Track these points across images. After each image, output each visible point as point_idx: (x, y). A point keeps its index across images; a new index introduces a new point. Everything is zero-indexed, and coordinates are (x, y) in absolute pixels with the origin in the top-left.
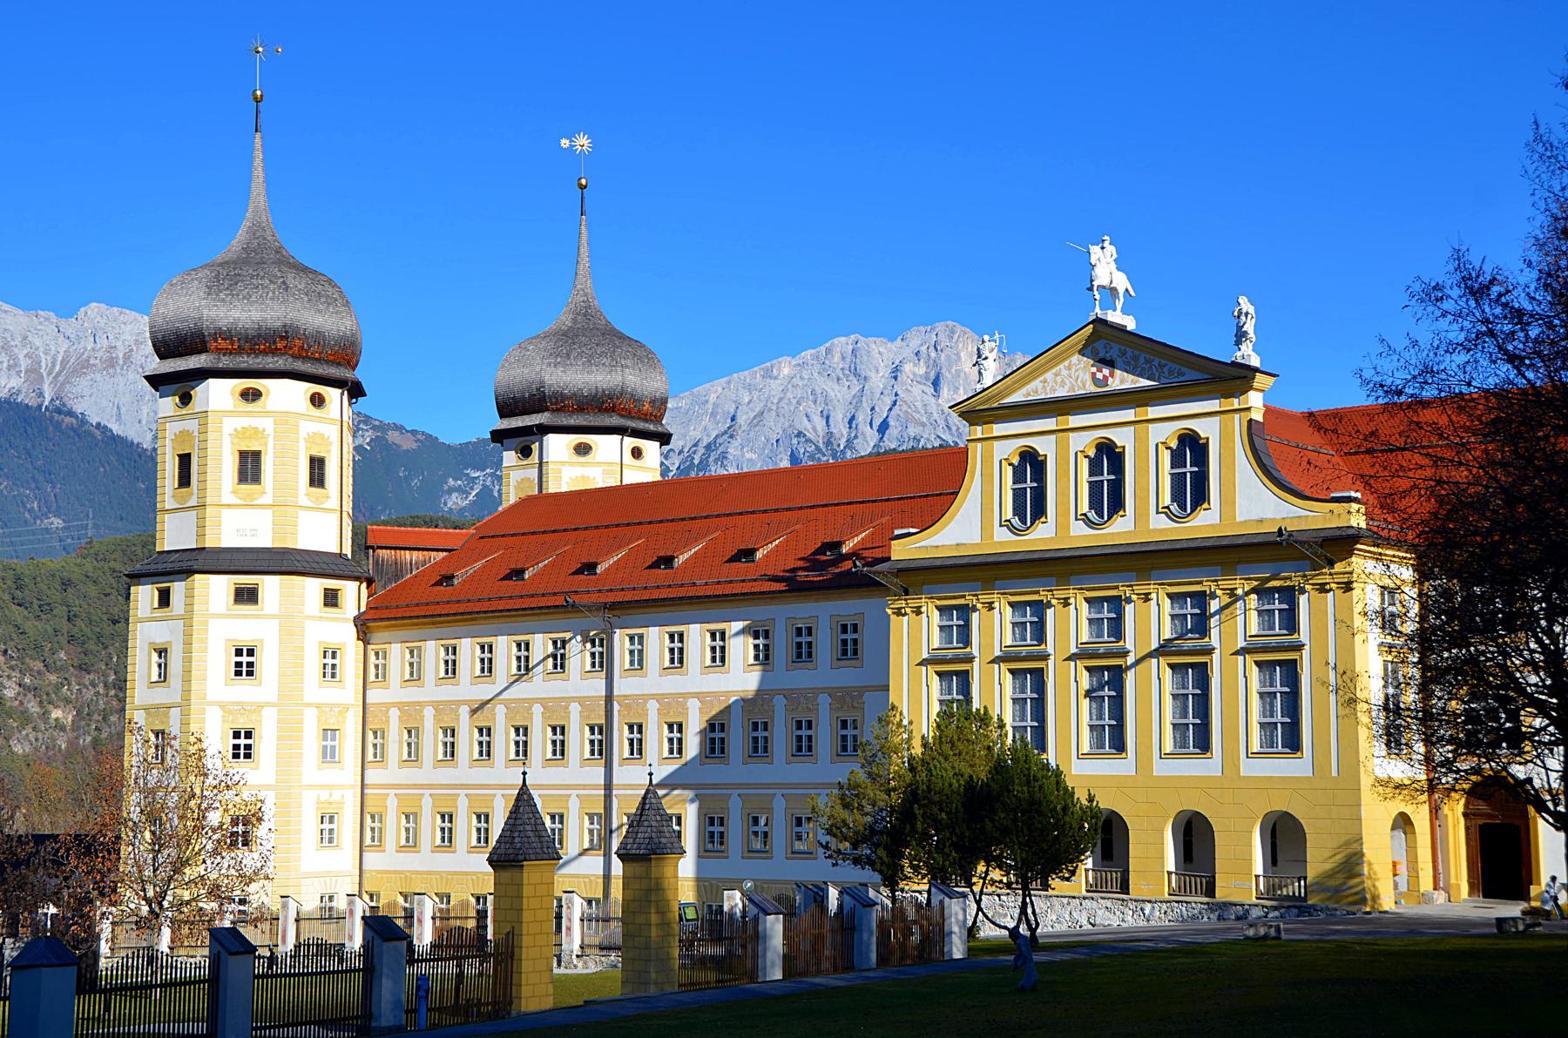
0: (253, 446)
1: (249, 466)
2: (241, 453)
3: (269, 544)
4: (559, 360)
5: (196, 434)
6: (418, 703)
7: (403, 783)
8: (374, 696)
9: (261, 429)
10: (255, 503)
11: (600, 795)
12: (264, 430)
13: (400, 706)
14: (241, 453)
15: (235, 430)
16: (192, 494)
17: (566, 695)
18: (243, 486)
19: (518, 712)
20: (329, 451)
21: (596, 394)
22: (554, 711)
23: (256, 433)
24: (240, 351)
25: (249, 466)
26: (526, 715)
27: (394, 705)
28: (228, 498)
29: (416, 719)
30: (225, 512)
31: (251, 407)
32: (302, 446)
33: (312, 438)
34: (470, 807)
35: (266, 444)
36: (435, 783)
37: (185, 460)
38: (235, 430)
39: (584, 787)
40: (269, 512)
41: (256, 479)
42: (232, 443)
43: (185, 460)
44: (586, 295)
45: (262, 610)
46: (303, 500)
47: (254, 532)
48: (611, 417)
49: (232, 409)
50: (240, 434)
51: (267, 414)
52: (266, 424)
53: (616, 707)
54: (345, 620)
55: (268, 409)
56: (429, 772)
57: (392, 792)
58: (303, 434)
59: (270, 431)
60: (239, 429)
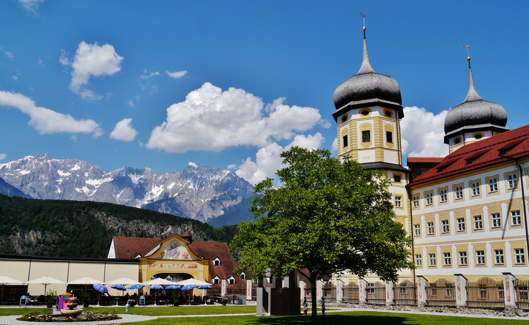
1: (366, 136)
2: (363, 132)
3: (375, 161)
5: (349, 128)
6: (432, 213)
7: (428, 243)
8: (414, 213)
11: (524, 240)
13: (425, 215)
14: (363, 132)
16: (348, 148)
17: (499, 200)
19: (476, 210)
20: (393, 130)
21: (482, 117)
22: (493, 208)
25: (366, 136)
26: (480, 211)
27: (423, 215)
28: (360, 147)
29: (432, 219)
30: (359, 152)
31: (366, 117)
32: (384, 128)
33: (386, 126)
34: (457, 250)
35: (371, 128)
36: (441, 241)
37: (345, 138)
39: (512, 238)
40: (374, 151)
41: (369, 140)
42: (360, 129)
43: (345, 138)
47: (369, 158)
50: (362, 126)
51: (371, 118)
53: (526, 202)
56: (439, 237)
57: (424, 246)
60: (362, 124)
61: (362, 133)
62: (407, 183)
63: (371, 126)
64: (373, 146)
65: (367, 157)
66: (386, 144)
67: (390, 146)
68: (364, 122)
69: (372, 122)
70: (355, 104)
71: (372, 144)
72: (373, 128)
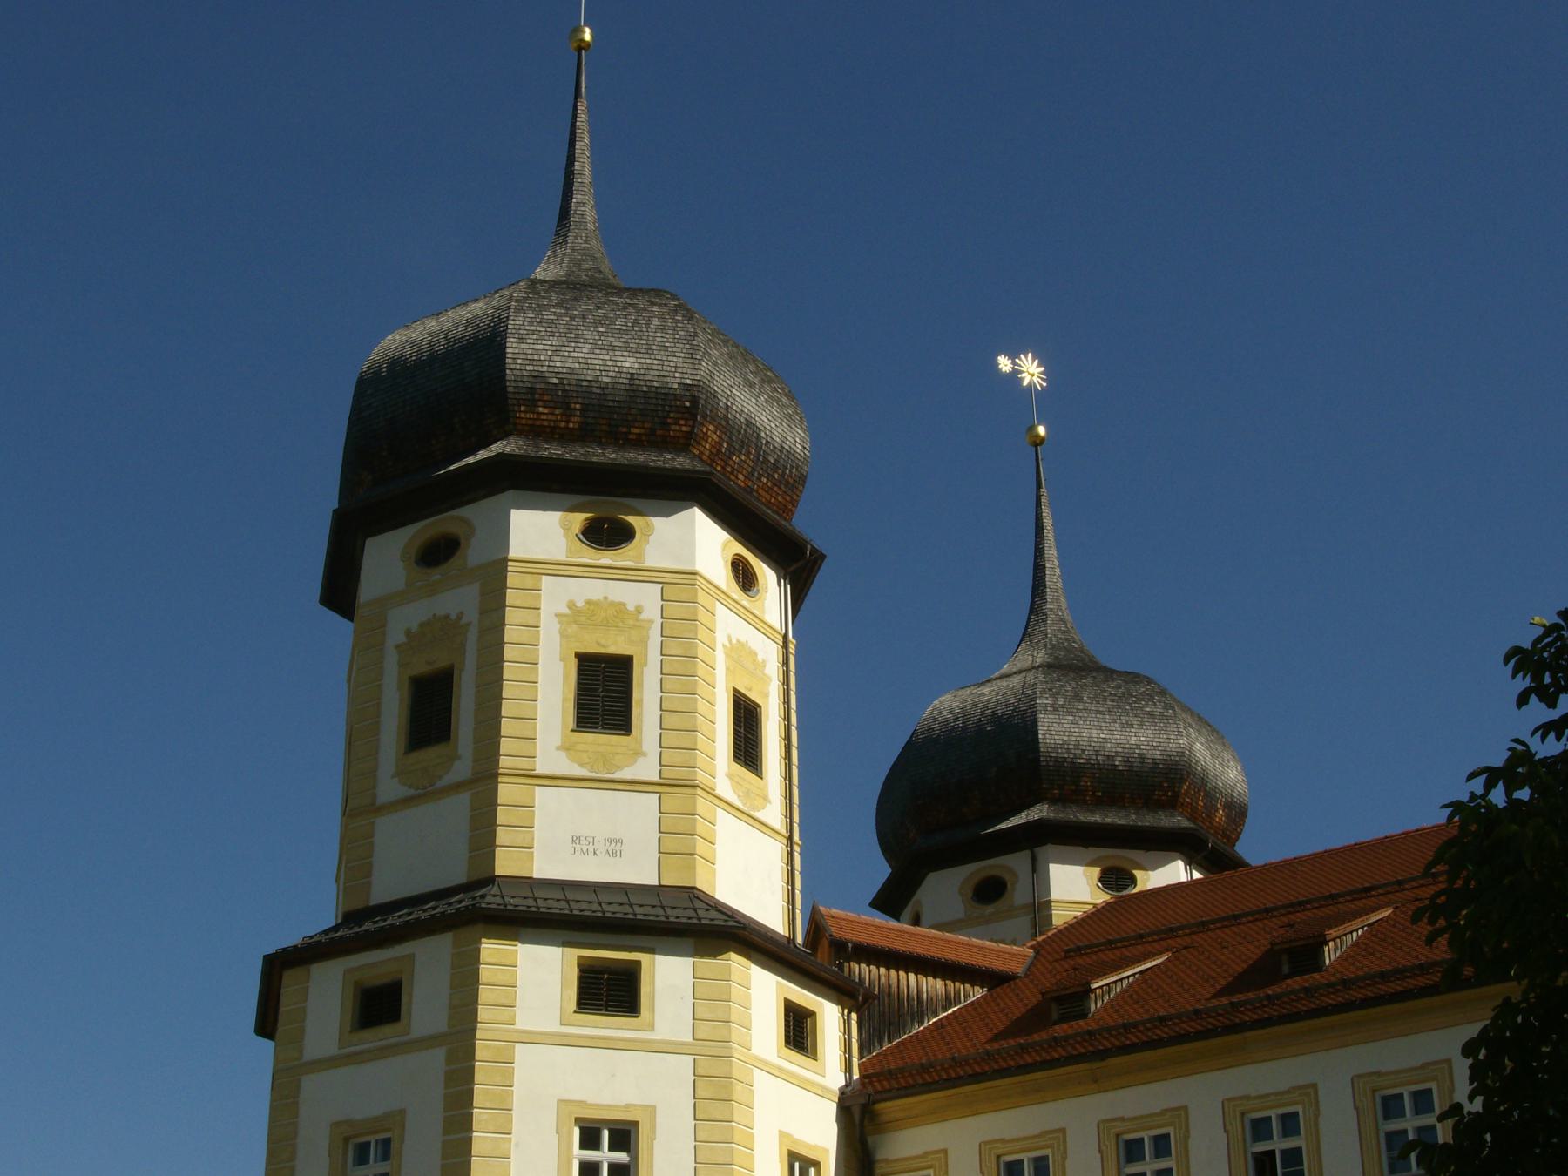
0: (614, 645)
4: (1061, 701)
9: (631, 607)
10: (617, 776)
12: (639, 610)
15: (571, 605)
18: (589, 738)
23: (619, 615)
24: (584, 435)
30: (544, 796)
31: (606, 558)
35: (644, 642)
38: (571, 605)
42: (563, 635)
44: (1062, 620)
45: (652, 1028)
46: (724, 788)
47: (614, 847)
48: (1173, 816)
49: (562, 558)
52: (645, 599)
54: (822, 1092)
55: (648, 564)
58: (721, 639)
59: (652, 611)
60: (580, 604)
61: (573, 663)
62: (848, 1068)
63: (642, 626)
64: (647, 769)
65: (600, 846)
66: (730, 776)
67: (748, 793)
68: (595, 590)
69: (645, 599)
70: (545, 454)
71: (638, 753)
72: (655, 638)
